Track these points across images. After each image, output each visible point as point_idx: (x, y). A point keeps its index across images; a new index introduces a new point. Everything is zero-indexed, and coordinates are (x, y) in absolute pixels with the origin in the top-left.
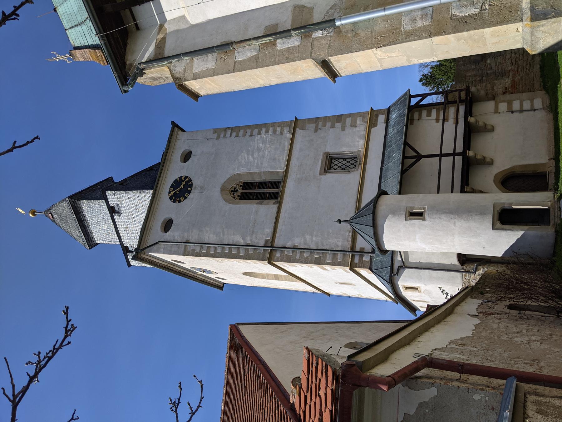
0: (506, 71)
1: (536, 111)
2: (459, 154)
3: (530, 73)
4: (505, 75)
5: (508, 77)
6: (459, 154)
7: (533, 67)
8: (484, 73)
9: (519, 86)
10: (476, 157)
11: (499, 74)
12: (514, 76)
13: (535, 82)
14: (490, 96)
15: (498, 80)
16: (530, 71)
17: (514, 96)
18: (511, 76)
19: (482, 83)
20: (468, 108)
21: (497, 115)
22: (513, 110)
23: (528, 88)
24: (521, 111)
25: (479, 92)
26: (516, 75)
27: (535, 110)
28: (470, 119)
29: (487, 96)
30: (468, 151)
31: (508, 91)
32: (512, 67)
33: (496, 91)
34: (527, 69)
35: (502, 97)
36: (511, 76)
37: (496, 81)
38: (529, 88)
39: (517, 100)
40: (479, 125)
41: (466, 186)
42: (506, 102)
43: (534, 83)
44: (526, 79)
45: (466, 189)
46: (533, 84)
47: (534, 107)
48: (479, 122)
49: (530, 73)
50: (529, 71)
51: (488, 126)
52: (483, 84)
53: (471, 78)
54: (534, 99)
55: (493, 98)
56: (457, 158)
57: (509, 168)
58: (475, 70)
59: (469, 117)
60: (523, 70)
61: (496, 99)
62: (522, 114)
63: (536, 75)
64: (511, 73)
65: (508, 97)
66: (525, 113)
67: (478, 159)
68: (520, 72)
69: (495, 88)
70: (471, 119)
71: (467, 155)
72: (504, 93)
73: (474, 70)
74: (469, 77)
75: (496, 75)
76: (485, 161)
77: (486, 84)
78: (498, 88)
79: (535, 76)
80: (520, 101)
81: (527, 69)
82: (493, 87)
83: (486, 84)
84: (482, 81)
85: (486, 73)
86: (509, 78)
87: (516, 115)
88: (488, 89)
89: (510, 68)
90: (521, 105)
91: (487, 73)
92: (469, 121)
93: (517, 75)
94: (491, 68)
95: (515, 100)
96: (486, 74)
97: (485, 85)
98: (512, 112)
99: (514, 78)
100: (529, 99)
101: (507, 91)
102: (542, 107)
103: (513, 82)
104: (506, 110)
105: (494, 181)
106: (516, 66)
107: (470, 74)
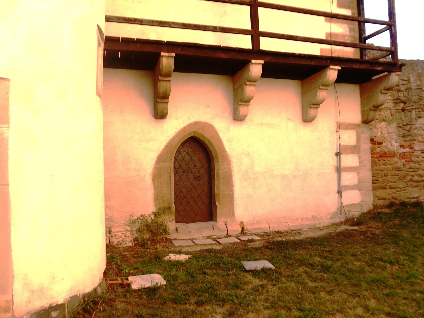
0: (412, 142)
1: (337, 194)
2: (255, 42)
3: (406, 182)
4: (406, 141)
5: (401, 146)
6: (255, 42)
7: (416, 186)
8: (412, 104)
9: (383, 164)
10: (247, 83)
11: (408, 131)
12: (403, 156)
13: (388, 190)
14: (372, 114)
15: (397, 129)
16: (408, 181)
17: (368, 156)
18: (402, 150)
19: (393, 103)
20: (357, 67)
21: (334, 127)
22: (343, 156)
23: (379, 179)
24: (339, 170)
25: (385, 92)
26: (403, 159)
27: (339, 192)
28: (335, 69)
29: (372, 109)
30: (262, 62)
31: (376, 146)
32: (419, 152)
33: (378, 126)
34: (413, 176)
35: (366, 135)
36: (402, 150)
37: (395, 125)
38: (378, 181)
39: (360, 162)
40: (318, 91)
41: (174, 55)
42: (357, 143)
43: (386, 189)
44: (395, 176)
45: (166, 54)
46: (384, 188)
47: (345, 190)
48: (326, 91)
49: (406, 182)
50: (409, 180)
51: (315, 110)
52: (392, 104)
53: (404, 82)
54: (360, 190)
55: (366, 122)
56: (249, 38)
57: (225, 151)
58: (418, 89)
59: (340, 68)
60: (410, 170)
61: (365, 125)
62: (333, 171)
63: (401, 191)
64: (408, 150)
65: (367, 146)
66: (335, 176)
67: (245, 87)
68: (408, 166)
69: (383, 124)
70: (334, 71)
71: (253, 61)
72: (372, 141)
73: (419, 87)
74: (405, 79)
75: (407, 125)
76: (240, 103)
77: (390, 109)
78: (382, 130)
79: (400, 190)
80: (358, 167)
81: (413, 176)
82: (384, 121)
83: (390, 109)
84: (398, 101)
85: (411, 108)
86: (399, 148)
87: (333, 161)
88: (382, 113)
89: (416, 148)
90: (350, 169)
91: (410, 111)
92: (331, 67)
93: (404, 161)
94: (420, 117)
95: (360, 158)
96: (409, 108)
97: (390, 107)
98: (338, 154)
99: (398, 156)
100: (360, 181)
101: (375, 144)
102: (344, 204)
103: (392, 155)
104: (342, 144)
105: (196, 123)
106: (419, 159)
107: (412, 80)
